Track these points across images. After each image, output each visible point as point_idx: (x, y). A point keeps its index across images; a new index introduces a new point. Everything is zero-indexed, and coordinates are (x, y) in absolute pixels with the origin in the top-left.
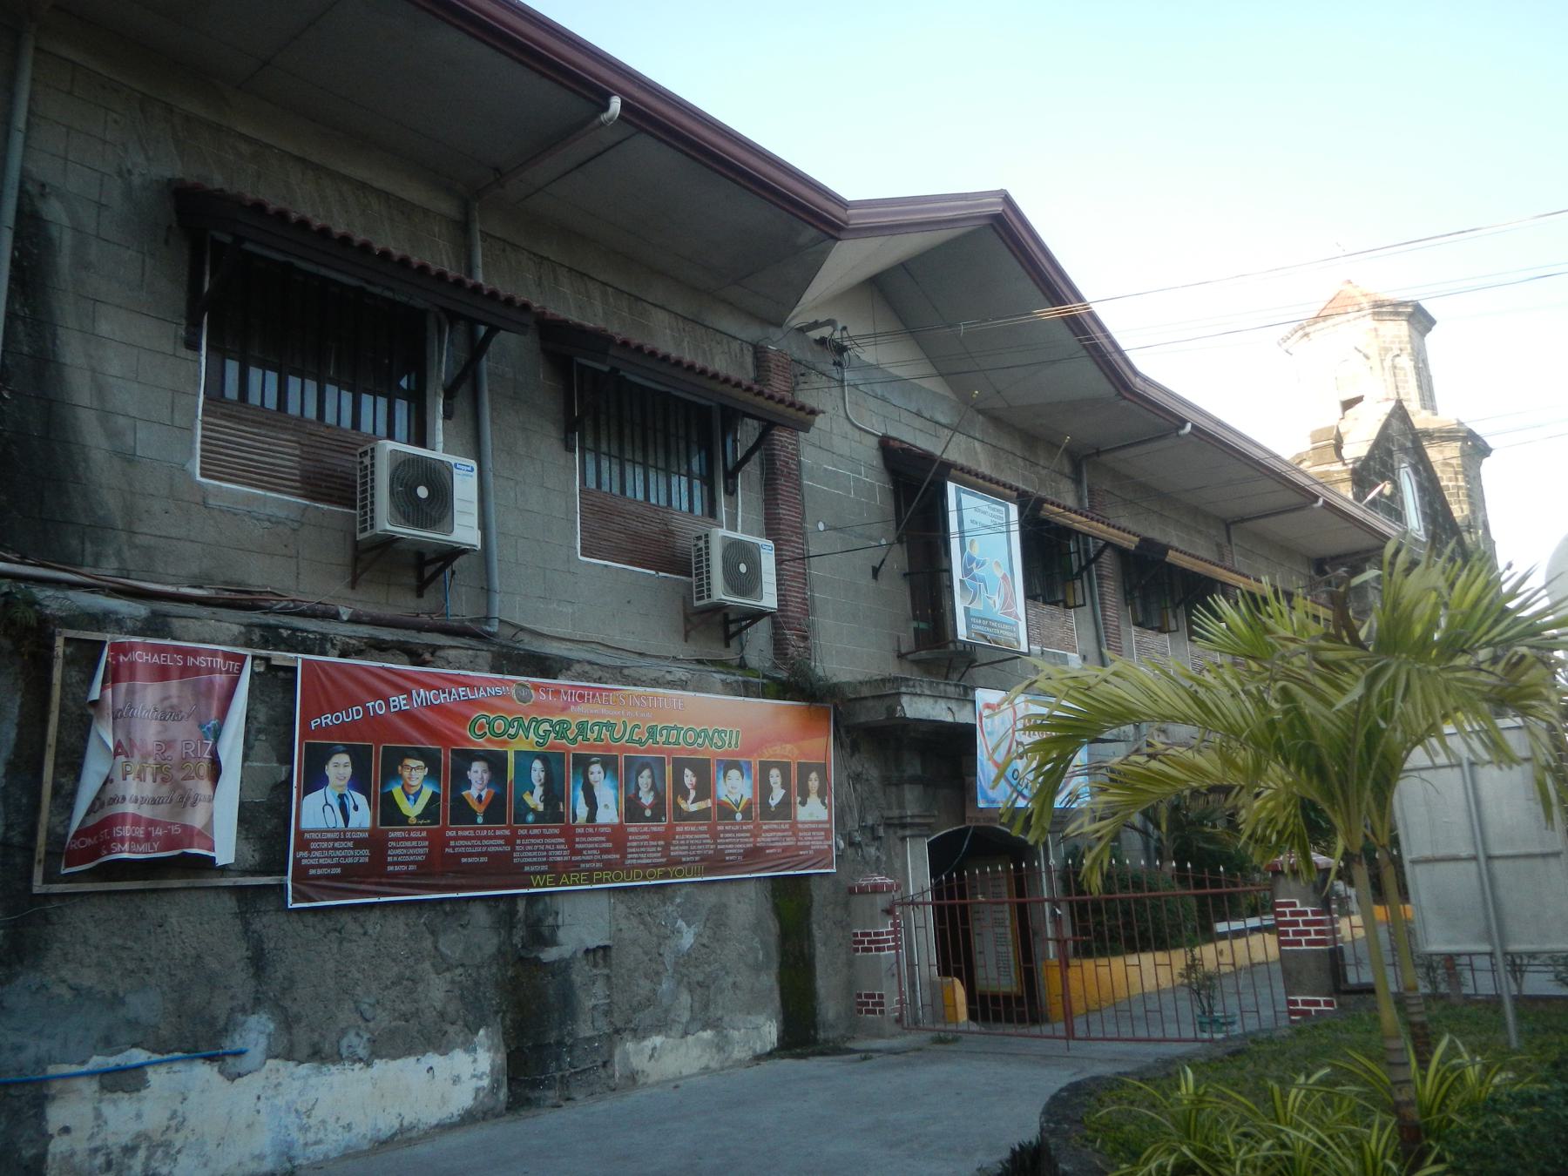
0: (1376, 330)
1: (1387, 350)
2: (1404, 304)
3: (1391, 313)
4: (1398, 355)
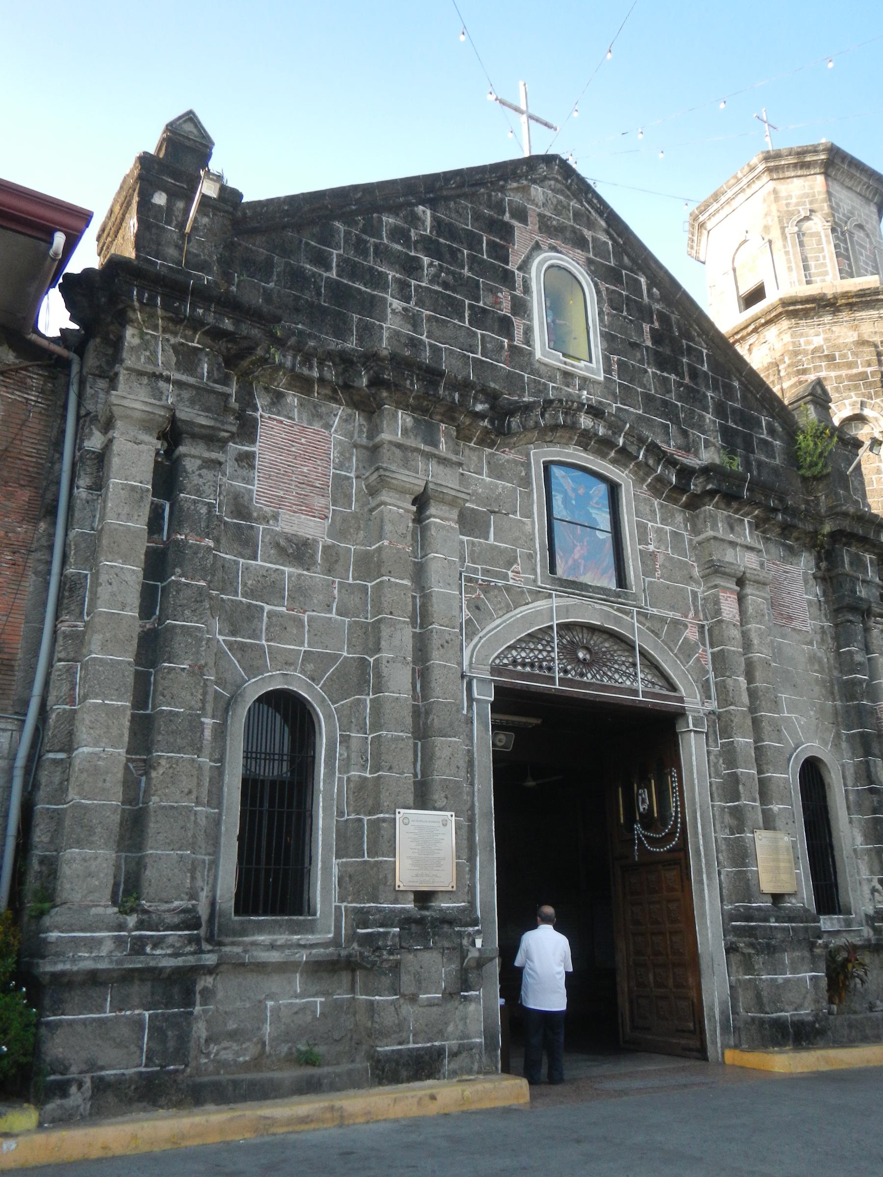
0: (775, 191)
1: (790, 214)
2: (815, 150)
3: (795, 165)
4: (807, 218)
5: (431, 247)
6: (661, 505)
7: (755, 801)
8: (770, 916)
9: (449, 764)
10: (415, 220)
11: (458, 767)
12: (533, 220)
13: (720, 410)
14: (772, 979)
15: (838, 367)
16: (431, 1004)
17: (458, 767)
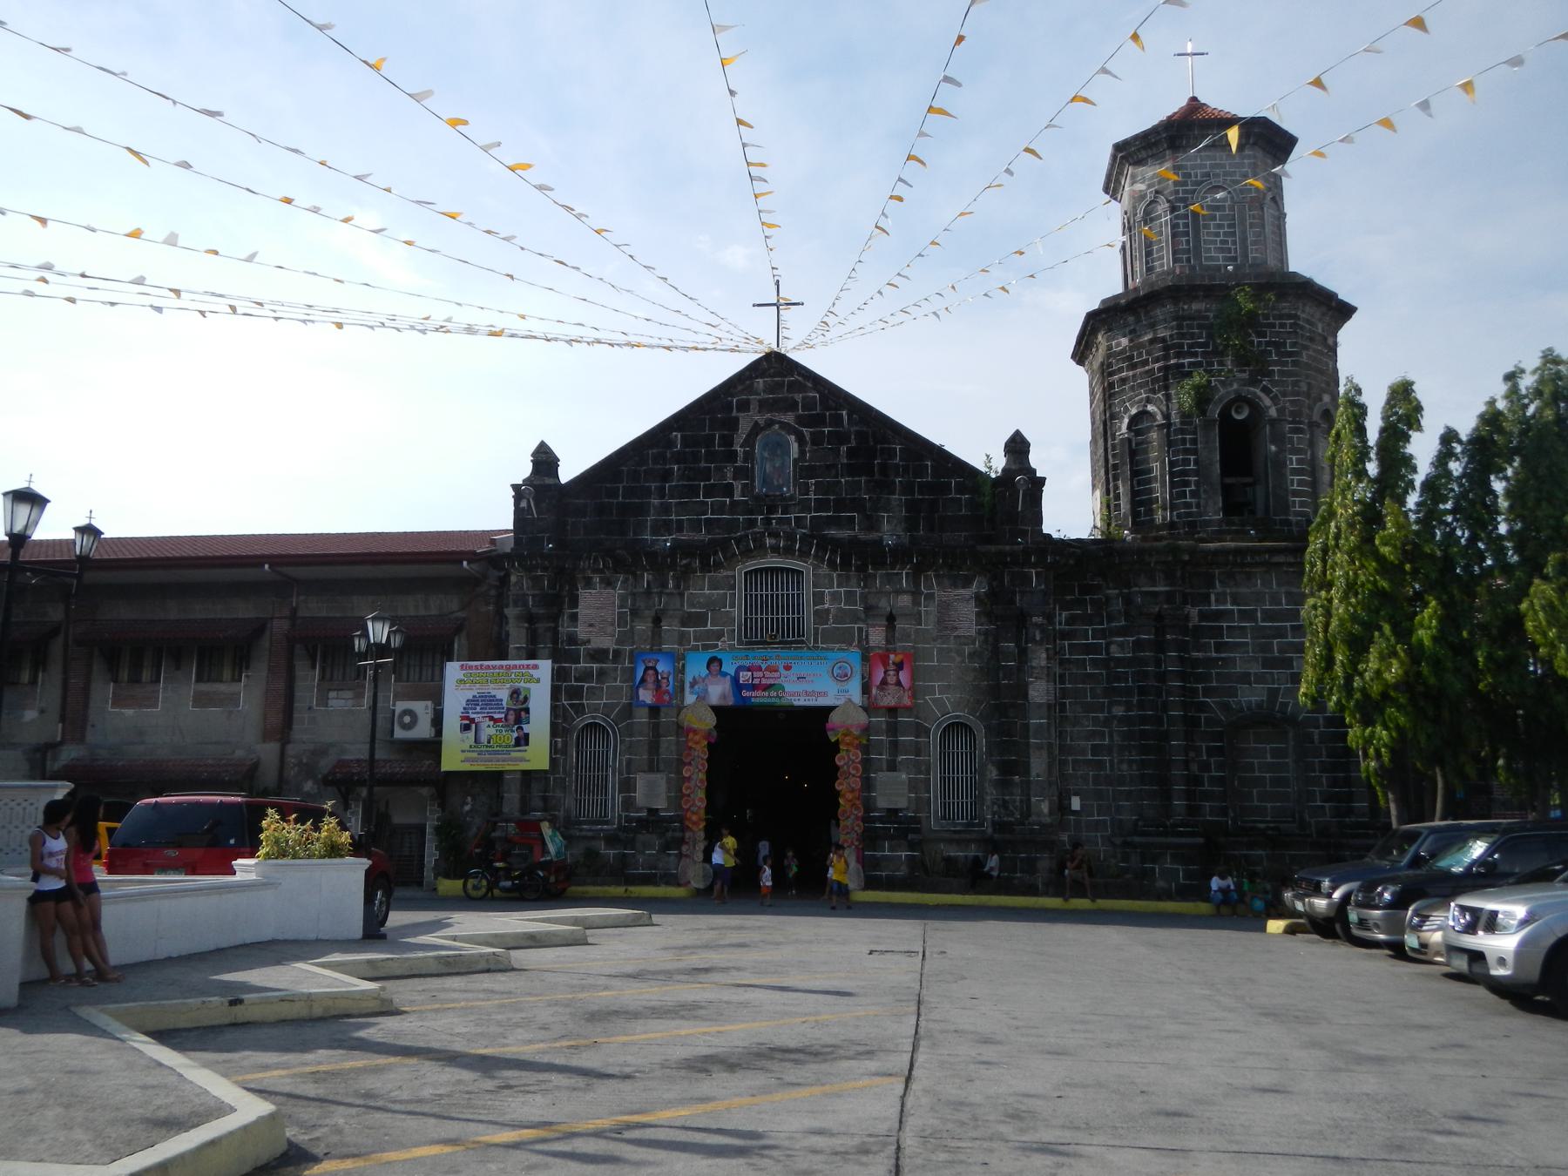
5: (679, 458)
6: (838, 575)
10: (671, 444)
12: (754, 406)
13: (908, 488)
15: (1133, 367)
16: (650, 855)
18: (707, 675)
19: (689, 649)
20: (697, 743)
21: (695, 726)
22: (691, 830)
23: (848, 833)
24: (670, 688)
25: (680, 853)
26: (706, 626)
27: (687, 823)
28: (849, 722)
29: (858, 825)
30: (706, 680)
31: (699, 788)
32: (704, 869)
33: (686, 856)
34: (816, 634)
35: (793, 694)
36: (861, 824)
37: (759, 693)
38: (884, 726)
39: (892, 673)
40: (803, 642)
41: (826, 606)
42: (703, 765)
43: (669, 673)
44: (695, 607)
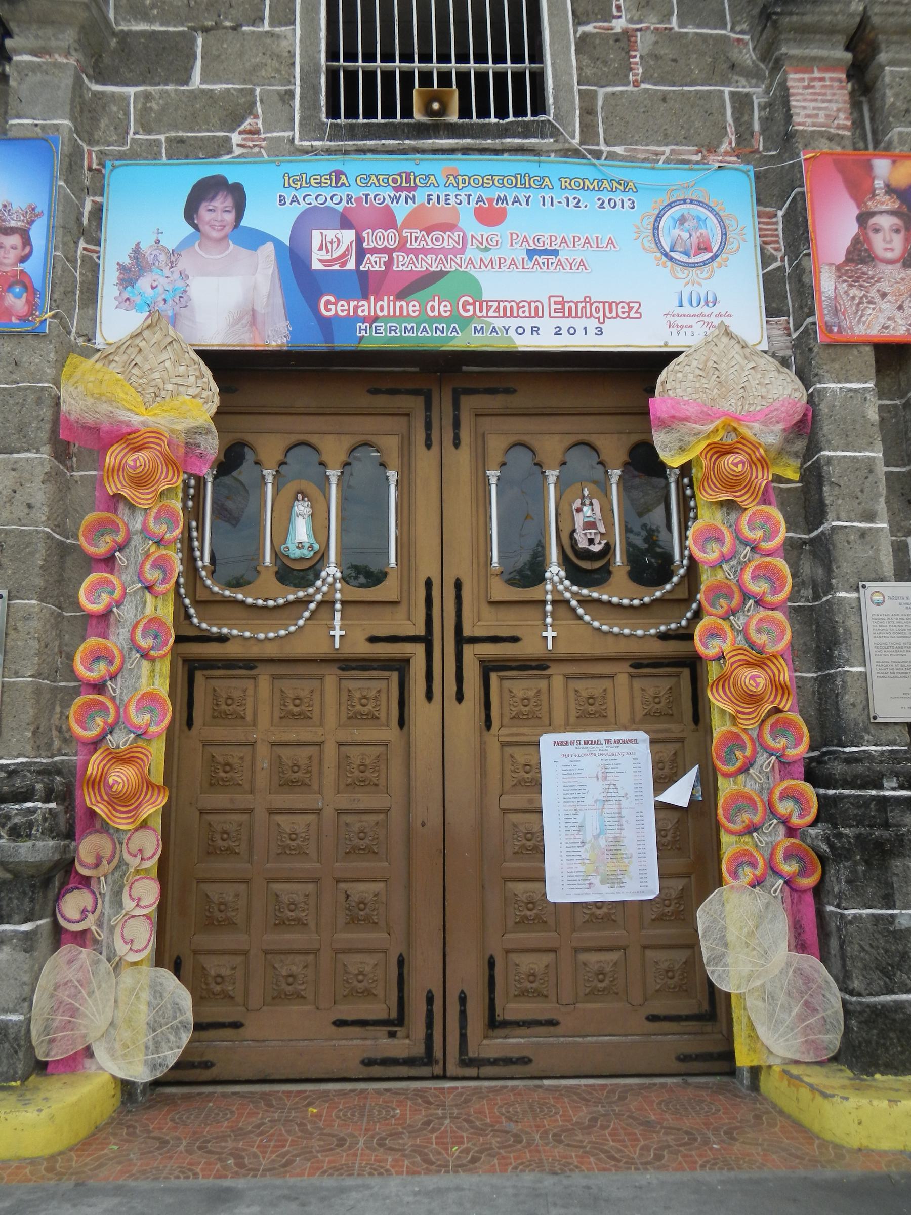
7: (870, 517)
8: (882, 775)
9: (10, 501)
11: (30, 506)
14: (876, 918)
17: (30, 506)
18: (186, 243)
19: (121, 156)
20: (140, 481)
21: (136, 420)
22: (105, 828)
23: (751, 829)
24: (34, 267)
25: (55, 923)
26: (187, 81)
27: (91, 800)
28: (731, 405)
29: (798, 798)
30: (183, 263)
31: (145, 655)
32: (157, 991)
33: (81, 938)
34: (588, 112)
35: (510, 310)
36: (808, 788)
37: (384, 306)
38: (873, 415)
39: (886, 222)
40: (541, 130)
41: (619, 25)
42: (161, 564)
43: (32, 215)
44: (145, 17)
